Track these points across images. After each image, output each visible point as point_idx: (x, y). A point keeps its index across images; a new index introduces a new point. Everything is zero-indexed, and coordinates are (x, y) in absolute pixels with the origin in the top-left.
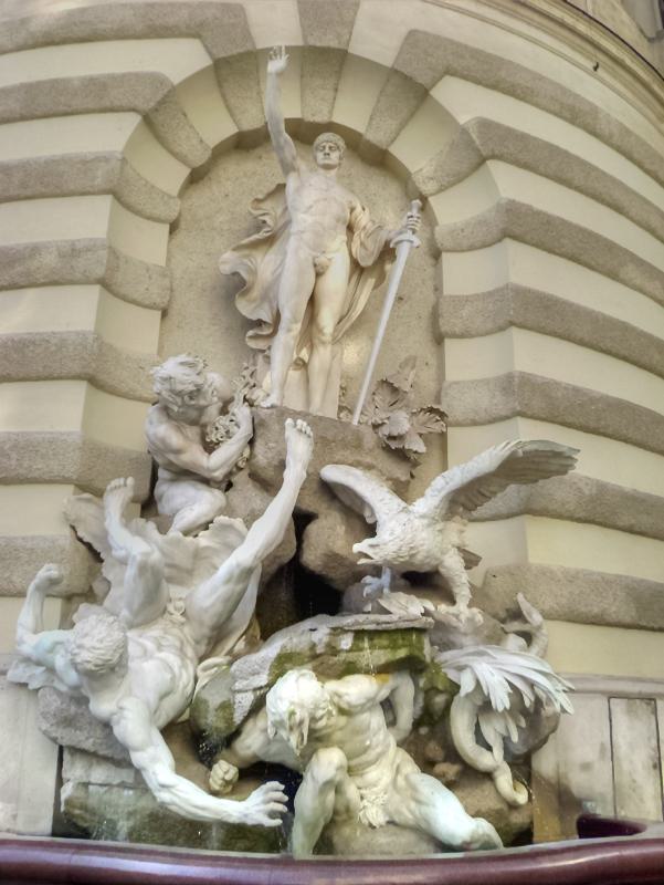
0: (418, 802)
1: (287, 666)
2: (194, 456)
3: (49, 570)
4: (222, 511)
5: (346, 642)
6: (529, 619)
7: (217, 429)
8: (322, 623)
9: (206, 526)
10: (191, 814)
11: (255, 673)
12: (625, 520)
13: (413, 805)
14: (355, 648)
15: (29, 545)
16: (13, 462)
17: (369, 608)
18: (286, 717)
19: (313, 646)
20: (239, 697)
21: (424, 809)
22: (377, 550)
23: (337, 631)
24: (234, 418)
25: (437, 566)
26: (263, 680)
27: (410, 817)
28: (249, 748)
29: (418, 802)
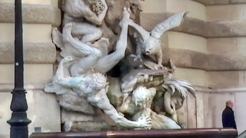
0: (163, 122)
1: (138, 85)
2: (93, 17)
3: (69, 58)
4: (103, 35)
5: (152, 79)
6: (172, 67)
7: (96, 7)
8: (145, 73)
9: (97, 40)
10: (127, 125)
11: (130, 88)
12: (190, 30)
13: (161, 124)
14: (153, 80)
15: (42, 46)
16: (32, 16)
17: (141, 66)
18: (144, 100)
19: (145, 80)
20: (125, 94)
21: (165, 124)
22: (151, 50)
23: (150, 76)
24: (101, 3)
25: (157, 53)
26: (131, 90)
27: (160, 126)
28: (125, 108)
29: (163, 122)
